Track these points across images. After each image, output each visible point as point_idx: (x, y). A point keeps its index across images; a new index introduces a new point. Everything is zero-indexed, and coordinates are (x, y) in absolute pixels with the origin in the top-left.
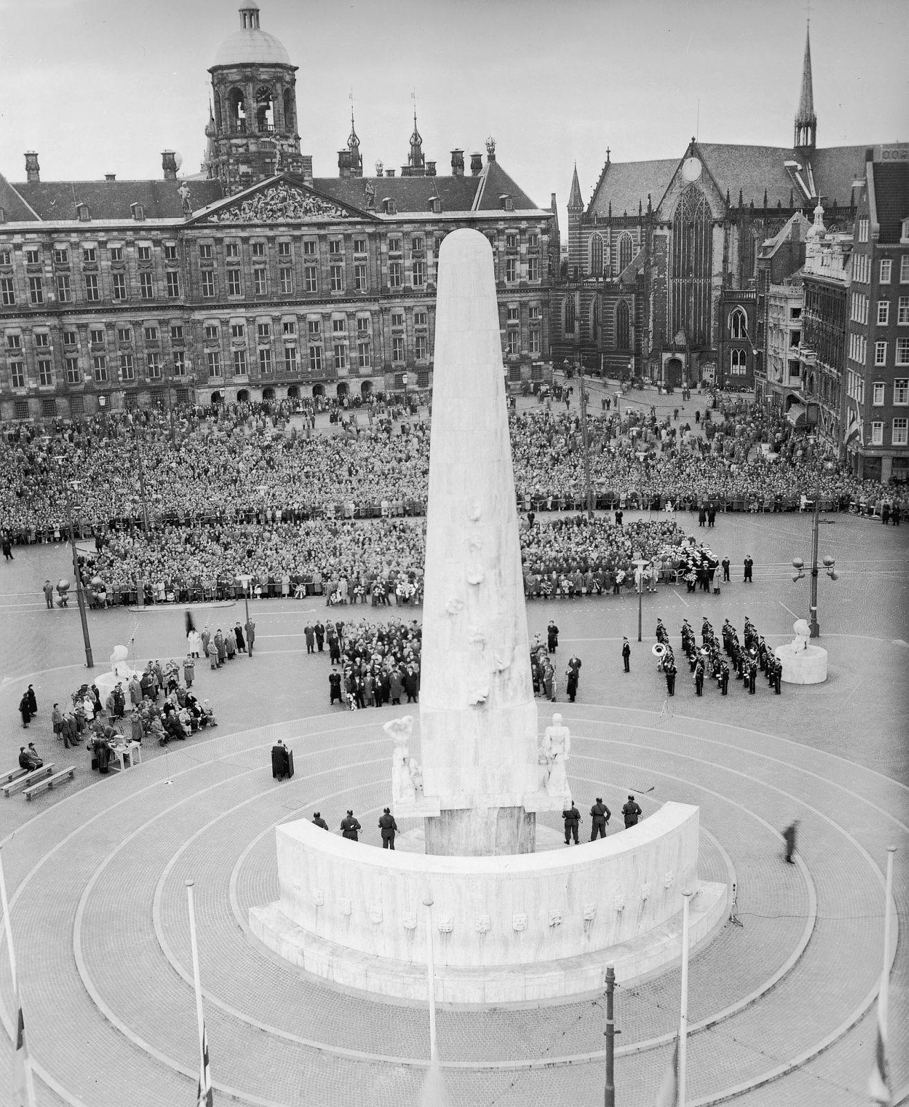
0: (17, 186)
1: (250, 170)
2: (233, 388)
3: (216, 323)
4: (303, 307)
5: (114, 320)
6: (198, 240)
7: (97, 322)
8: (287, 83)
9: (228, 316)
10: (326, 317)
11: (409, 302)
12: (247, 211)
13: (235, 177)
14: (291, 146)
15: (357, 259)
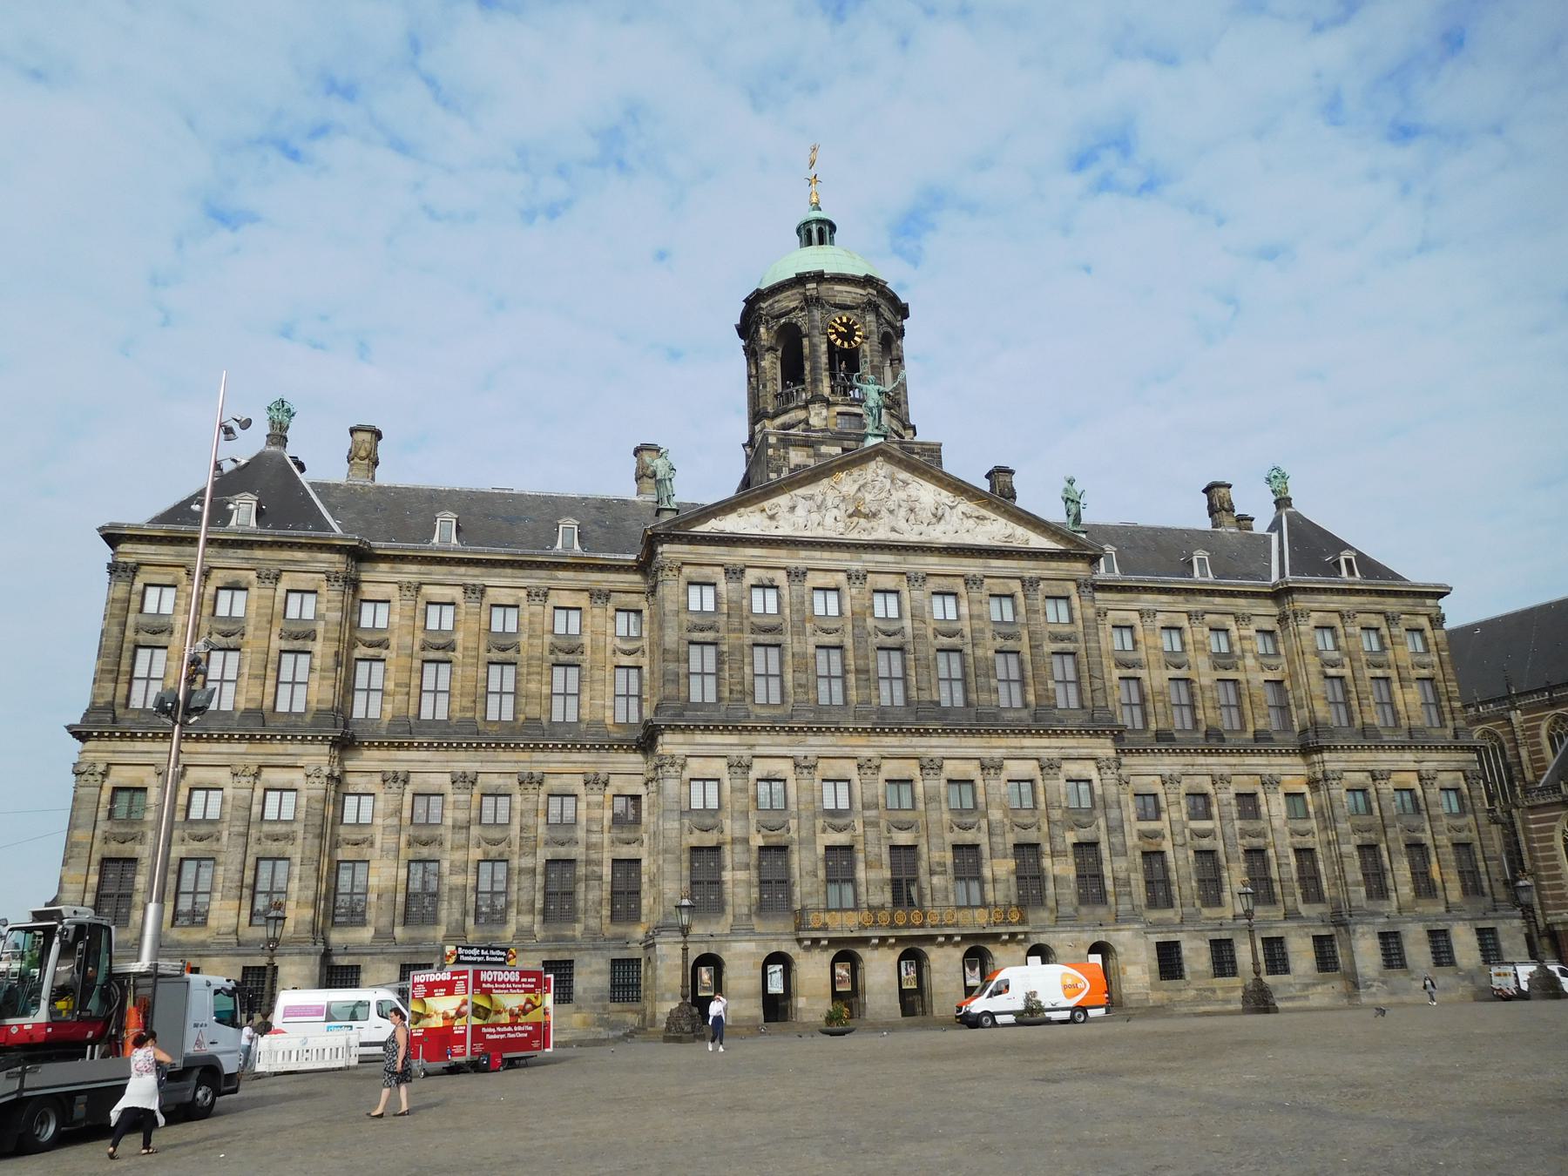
0: (312, 485)
1: (811, 462)
2: (751, 946)
3: (718, 767)
4: (934, 741)
5: (476, 767)
6: (686, 570)
7: (432, 769)
8: (889, 323)
9: (746, 753)
10: (990, 767)
11: (1170, 764)
12: (800, 511)
13: (779, 471)
14: (896, 432)
15: (1056, 638)
